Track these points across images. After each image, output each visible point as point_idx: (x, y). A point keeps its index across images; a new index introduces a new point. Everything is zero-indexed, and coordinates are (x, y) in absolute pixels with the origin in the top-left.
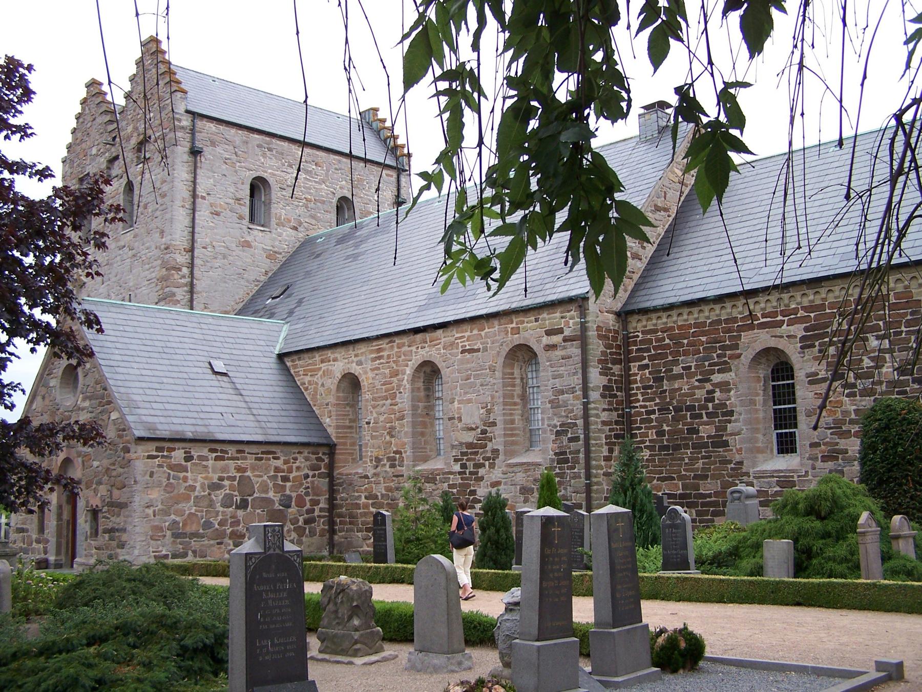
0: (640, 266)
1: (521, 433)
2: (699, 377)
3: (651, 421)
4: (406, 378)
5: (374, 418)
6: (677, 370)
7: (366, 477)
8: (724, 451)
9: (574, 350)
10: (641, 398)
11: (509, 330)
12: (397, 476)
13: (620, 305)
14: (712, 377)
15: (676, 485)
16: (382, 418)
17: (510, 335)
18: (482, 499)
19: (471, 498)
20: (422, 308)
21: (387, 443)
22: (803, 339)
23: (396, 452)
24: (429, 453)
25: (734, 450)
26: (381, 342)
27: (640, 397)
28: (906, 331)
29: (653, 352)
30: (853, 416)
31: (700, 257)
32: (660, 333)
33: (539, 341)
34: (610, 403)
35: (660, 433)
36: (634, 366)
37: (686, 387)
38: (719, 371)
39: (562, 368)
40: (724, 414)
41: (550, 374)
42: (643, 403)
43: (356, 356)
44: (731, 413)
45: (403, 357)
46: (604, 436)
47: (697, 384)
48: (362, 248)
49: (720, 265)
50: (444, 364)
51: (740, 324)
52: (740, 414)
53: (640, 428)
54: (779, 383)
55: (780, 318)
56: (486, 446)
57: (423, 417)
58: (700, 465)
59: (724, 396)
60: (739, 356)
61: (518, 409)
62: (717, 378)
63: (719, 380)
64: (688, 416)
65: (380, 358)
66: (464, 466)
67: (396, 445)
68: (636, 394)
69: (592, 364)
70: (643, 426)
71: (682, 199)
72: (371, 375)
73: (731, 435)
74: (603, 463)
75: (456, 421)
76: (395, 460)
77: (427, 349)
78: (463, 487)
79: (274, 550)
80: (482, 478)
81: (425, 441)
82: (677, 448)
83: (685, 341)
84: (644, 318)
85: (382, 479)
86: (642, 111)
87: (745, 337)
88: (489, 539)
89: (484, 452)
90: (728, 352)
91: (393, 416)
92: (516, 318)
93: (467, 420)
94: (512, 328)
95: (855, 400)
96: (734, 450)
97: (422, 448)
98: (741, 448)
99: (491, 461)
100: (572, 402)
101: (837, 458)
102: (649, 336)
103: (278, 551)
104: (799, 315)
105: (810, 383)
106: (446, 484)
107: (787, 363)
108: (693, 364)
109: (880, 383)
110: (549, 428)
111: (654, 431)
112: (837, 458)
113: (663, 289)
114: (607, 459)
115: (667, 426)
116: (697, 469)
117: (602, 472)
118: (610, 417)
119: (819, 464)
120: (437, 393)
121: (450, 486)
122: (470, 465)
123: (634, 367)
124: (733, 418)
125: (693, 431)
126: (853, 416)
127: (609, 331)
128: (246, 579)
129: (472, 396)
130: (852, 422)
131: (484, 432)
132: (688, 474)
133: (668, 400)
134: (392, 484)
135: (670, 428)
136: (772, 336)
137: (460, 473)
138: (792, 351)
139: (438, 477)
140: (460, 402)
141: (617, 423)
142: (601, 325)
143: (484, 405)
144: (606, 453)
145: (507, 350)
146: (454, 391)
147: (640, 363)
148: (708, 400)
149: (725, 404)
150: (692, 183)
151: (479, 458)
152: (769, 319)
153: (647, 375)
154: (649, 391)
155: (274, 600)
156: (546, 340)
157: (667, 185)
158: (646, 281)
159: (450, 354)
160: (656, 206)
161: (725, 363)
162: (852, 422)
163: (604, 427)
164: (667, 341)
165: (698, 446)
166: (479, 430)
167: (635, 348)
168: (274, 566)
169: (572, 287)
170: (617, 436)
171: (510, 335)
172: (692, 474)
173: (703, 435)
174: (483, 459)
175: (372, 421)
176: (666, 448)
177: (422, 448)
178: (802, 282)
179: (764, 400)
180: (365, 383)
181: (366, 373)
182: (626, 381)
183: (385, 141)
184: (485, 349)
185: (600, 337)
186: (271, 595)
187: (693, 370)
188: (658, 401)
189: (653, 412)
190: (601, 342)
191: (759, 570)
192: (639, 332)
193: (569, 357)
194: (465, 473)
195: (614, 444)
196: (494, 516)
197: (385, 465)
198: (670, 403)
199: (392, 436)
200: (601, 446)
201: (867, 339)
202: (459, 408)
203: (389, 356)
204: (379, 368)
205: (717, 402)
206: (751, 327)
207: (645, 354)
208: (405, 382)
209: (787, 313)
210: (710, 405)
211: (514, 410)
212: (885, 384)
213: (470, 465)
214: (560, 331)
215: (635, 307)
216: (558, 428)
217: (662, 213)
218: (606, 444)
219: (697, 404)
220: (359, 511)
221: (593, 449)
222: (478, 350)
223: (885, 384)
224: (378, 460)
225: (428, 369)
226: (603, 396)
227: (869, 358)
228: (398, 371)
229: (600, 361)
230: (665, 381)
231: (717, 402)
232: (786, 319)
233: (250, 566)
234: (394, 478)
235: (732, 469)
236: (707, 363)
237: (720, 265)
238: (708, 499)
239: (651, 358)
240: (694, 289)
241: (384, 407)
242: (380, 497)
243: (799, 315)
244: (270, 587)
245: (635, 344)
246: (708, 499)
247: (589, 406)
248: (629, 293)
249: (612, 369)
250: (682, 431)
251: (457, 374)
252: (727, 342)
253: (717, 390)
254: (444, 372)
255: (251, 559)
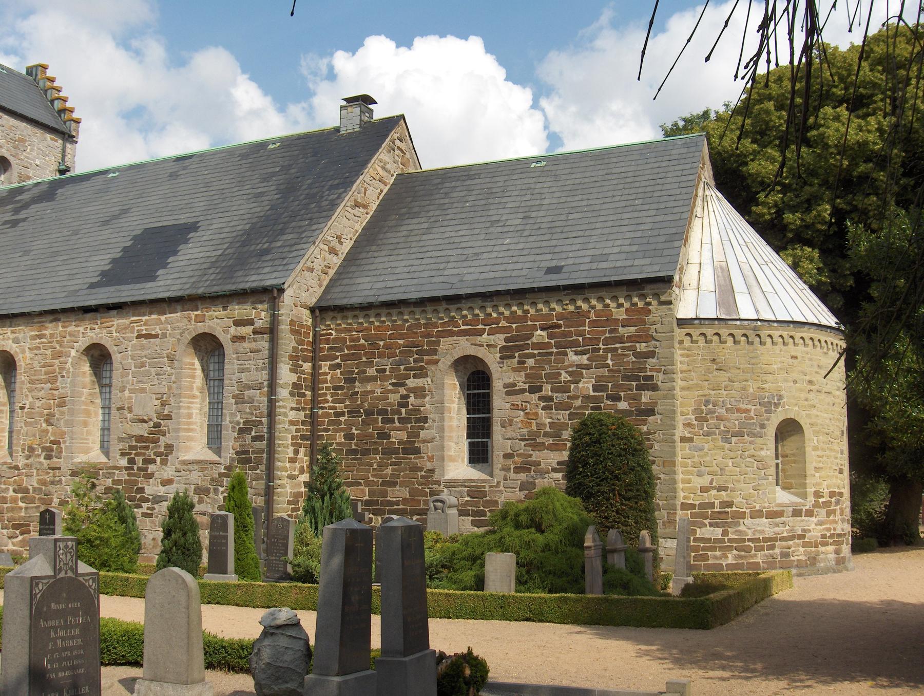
0: (336, 261)
1: (198, 428)
2: (394, 381)
3: (340, 423)
4: (70, 360)
5: (30, 402)
6: (371, 372)
7: (16, 468)
8: (414, 458)
9: (263, 344)
10: (330, 399)
11: (193, 317)
12: (53, 469)
13: (314, 300)
14: (407, 382)
15: (363, 491)
16: (38, 403)
17: (193, 322)
18: (151, 497)
19: (138, 496)
20: (92, 286)
21: (43, 431)
22: (503, 349)
23: (52, 442)
24: (91, 445)
25: (426, 458)
26: (44, 319)
27: (329, 398)
28: (604, 349)
29: (346, 352)
30: (548, 429)
31: (401, 257)
32: (354, 333)
33: (226, 331)
34: (298, 402)
35: (349, 437)
36: (325, 365)
37: (379, 390)
38: (415, 376)
39: (250, 362)
40: (418, 420)
41: (236, 367)
42: (332, 404)
43: (13, 332)
44: (425, 420)
45: (68, 338)
46: (290, 436)
47: (390, 387)
48: (23, 214)
49: (422, 268)
50: (115, 348)
51: (440, 329)
52: (434, 421)
53: (327, 430)
54: (474, 392)
55: (480, 326)
56: (158, 441)
57: (86, 404)
58: (389, 470)
59: (419, 401)
60: (436, 362)
61: (196, 403)
62: (412, 383)
63: (415, 385)
64: (380, 420)
65: (40, 337)
66: (132, 461)
67: (54, 434)
68: (326, 394)
69: (283, 359)
70: (331, 428)
71: (381, 197)
72: (28, 354)
73: (424, 441)
74: (288, 465)
75: (126, 412)
76: (52, 451)
77: (97, 331)
78: (130, 483)
79: (66, 573)
80: (151, 476)
81: (87, 431)
82: (366, 452)
83: (381, 343)
84: (339, 315)
85: (35, 471)
86: (344, 103)
87: (445, 343)
88: (175, 543)
89: (156, 447)
90: (425, 358)
91: (52, 402)
92: (202, 304)
93: (138, 411)
94: (196, 316)
95: (551, 413)
96: (426, 458)
97: (82, 439)
98: (433, 456)
99: (163, 457)
100: (258, 398)
101: (529, 470)
102: (343, 335)
103: (70, 574)
104: (500, 325)
105: (507, 393)
106: (110, 480)
107: (484, 373)
108: (388, 367)
109: (576, 397)
110: (231, 425)
111: (343, 434)
112: (529, 470)
113: (360, 287)
114: (292, 460)
115: (356, 430)
116: (386, 475)
117: (286, 474)
118: (298, 417)
119: (512, 475)
120: (104, 380)
121: (115, 482)
122: (139, 460)
123: (325, 366)
124: (426, 425)
125: (384, 436)
126: (548, 429)
127: (302, 326)
128: (31, 611)
129: (148, 386)
130: (546, 434)
131: (157, 425)
132: (376, 480)
133: (359, 402)
134: (46, 477)
135: (359, 432)
136: (472, 344)
137: (127, 468)
138: (492, 360)
139: (101, 472)
140: (131, 391)
141: (303, 423)
142: (295, 319)
143: (160, 396)
144: (291, 455)
145: (190, 338)
146: (125, 379)
147: (331, 363)
148: (401, 405)
149: (419, 410)
150: (391, 183)
151: (150, 453)
152: (470, 327)
153: (339, 375)
154: (340, 392)
155: (63, 639)
156: (233, 331)
157: (368, 181)
158: (342, 277)
159: (124, 338)
160: (355, 201)
161: (422, 368)
162: (546, 434)
163: (291, 427)
164: (362, 341)
165: (388, 452)
166: (152, 423)
167: (327, 346)
168: (65, 595)
169: (267, 276)
170: (303, 437)
171: (193, 322)
172: (381, 480)
173: (394, 440)
174: (155, 454)
175: (27, 406)
176: (354, 452)
177: (82, 439)
178: (507, 292)
179: (459, 409)
180: (23, 364)
181: (23, 352)
182: (315, 379)
183: (52, 101)
184: (164, 336)
185: (293, 332)
186: (62, 633)
187: (388, 373)
188: (348, 403)
189: (343, 414)
190: (293, 337)
191: (480, 583)
192: (332, 329)
193: (258, 351)
194: (132, 469)
195: (300, 445)
196: (180, 518)
197: (40, 455)
198: (361, 406)
199: (50, 424)
200: (287, 447)
201: (566, 354)
202: (130, 398)
203: (52, 335)
204: (40, 347)
205: (410, 407)
206: (451, 334)
207: (338, 354)
208: (69, 365)
209: (489, 322)
210: (403, 410)
211: (193, 403)
212: (580, 398)
213: (139, 460)
214: (250, 322)
215: (331, 303)
216: (241, 426)
217: (361, 210)
218: (293, 444)
219: (389, 409)
220: (5, 506)
221: (280, 449)
222: (156, 336)
223: (580, 398)
224: (31, 449)
225: (96, 353)
226: (292, 394)
227: (566, 372)
228: (62, 352)
229: (291, 358)
230: (357, 383)
231: (410, 407)
232: (487, 328)
233: (36, 595)
234: (51, 471)
235: (422, 477)
236: (402, 367)
237: (422, 268)
238: (395, 507)
239: (345, 358)
240: (396, 290)
241: (43, 391)
242: (31, 491)
243: (500, 325)
244: (60, 622)
245: (327, 341)
246: (395, 507)
247: (277, 404)
248: (323, 288)
249: (302, 366)
250: (371, 435)
251: (130, 361)
252: (425, 347)
253: (412, 395)
254: (116, 357)
255: (37, 584)
